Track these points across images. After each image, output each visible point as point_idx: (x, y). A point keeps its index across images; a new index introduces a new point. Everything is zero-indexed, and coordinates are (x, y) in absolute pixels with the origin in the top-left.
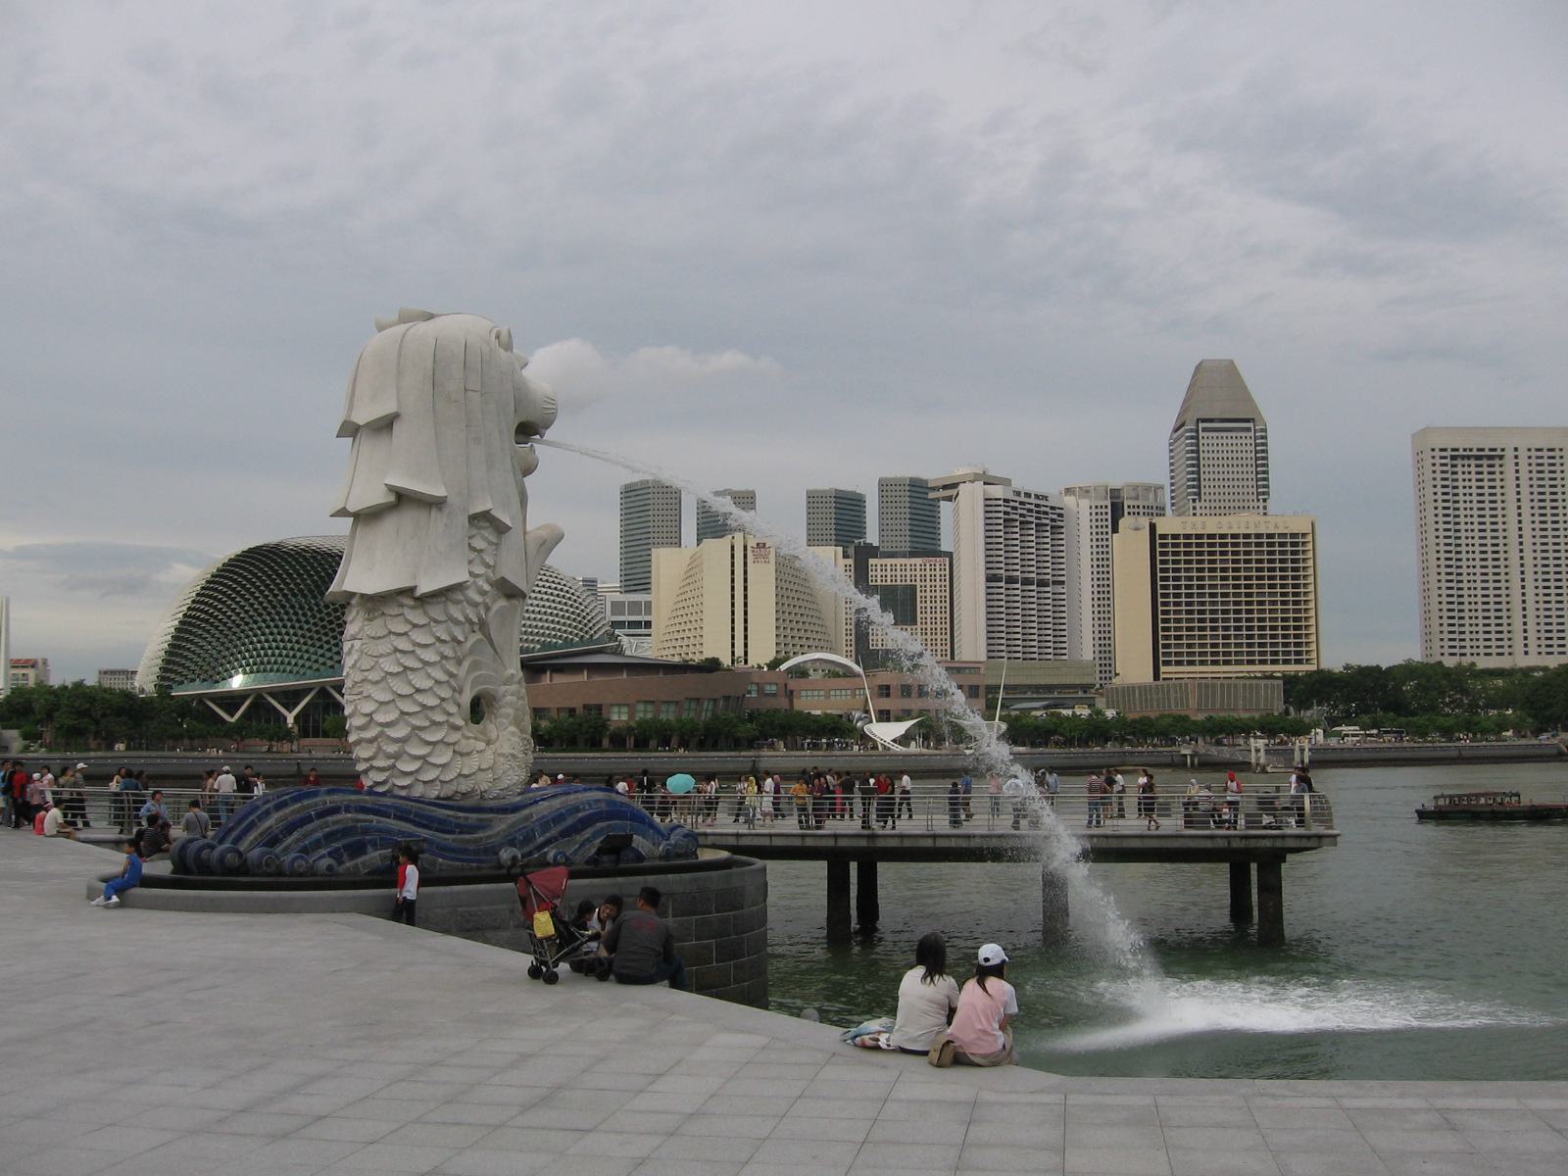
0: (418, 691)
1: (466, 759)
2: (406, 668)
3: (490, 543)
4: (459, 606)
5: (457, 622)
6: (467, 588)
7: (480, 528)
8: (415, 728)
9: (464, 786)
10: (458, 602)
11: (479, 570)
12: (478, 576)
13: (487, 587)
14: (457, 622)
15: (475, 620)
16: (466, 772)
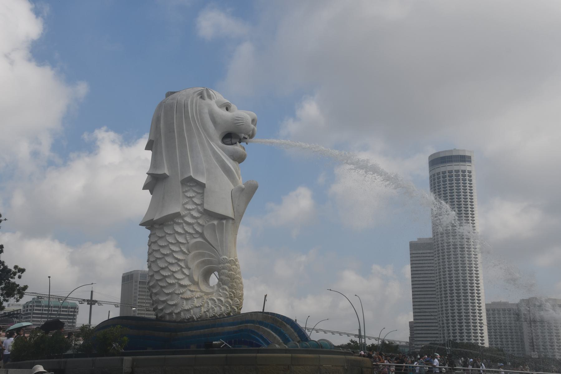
0: (162, 269)
1: (190, 302)
2: (157, 258)
3: (198, 193)
4: (181, 225)
5: (179, 234)
6: (184, 216)
7: (190, 186)
8: (162, 287)
9: (188, 316)
10: (178, 224)
11: (189, 206)
12: (190, 210)
13: (195, 214)
14: (179, 234)
15: (191, 231)
16: (187, 307)
